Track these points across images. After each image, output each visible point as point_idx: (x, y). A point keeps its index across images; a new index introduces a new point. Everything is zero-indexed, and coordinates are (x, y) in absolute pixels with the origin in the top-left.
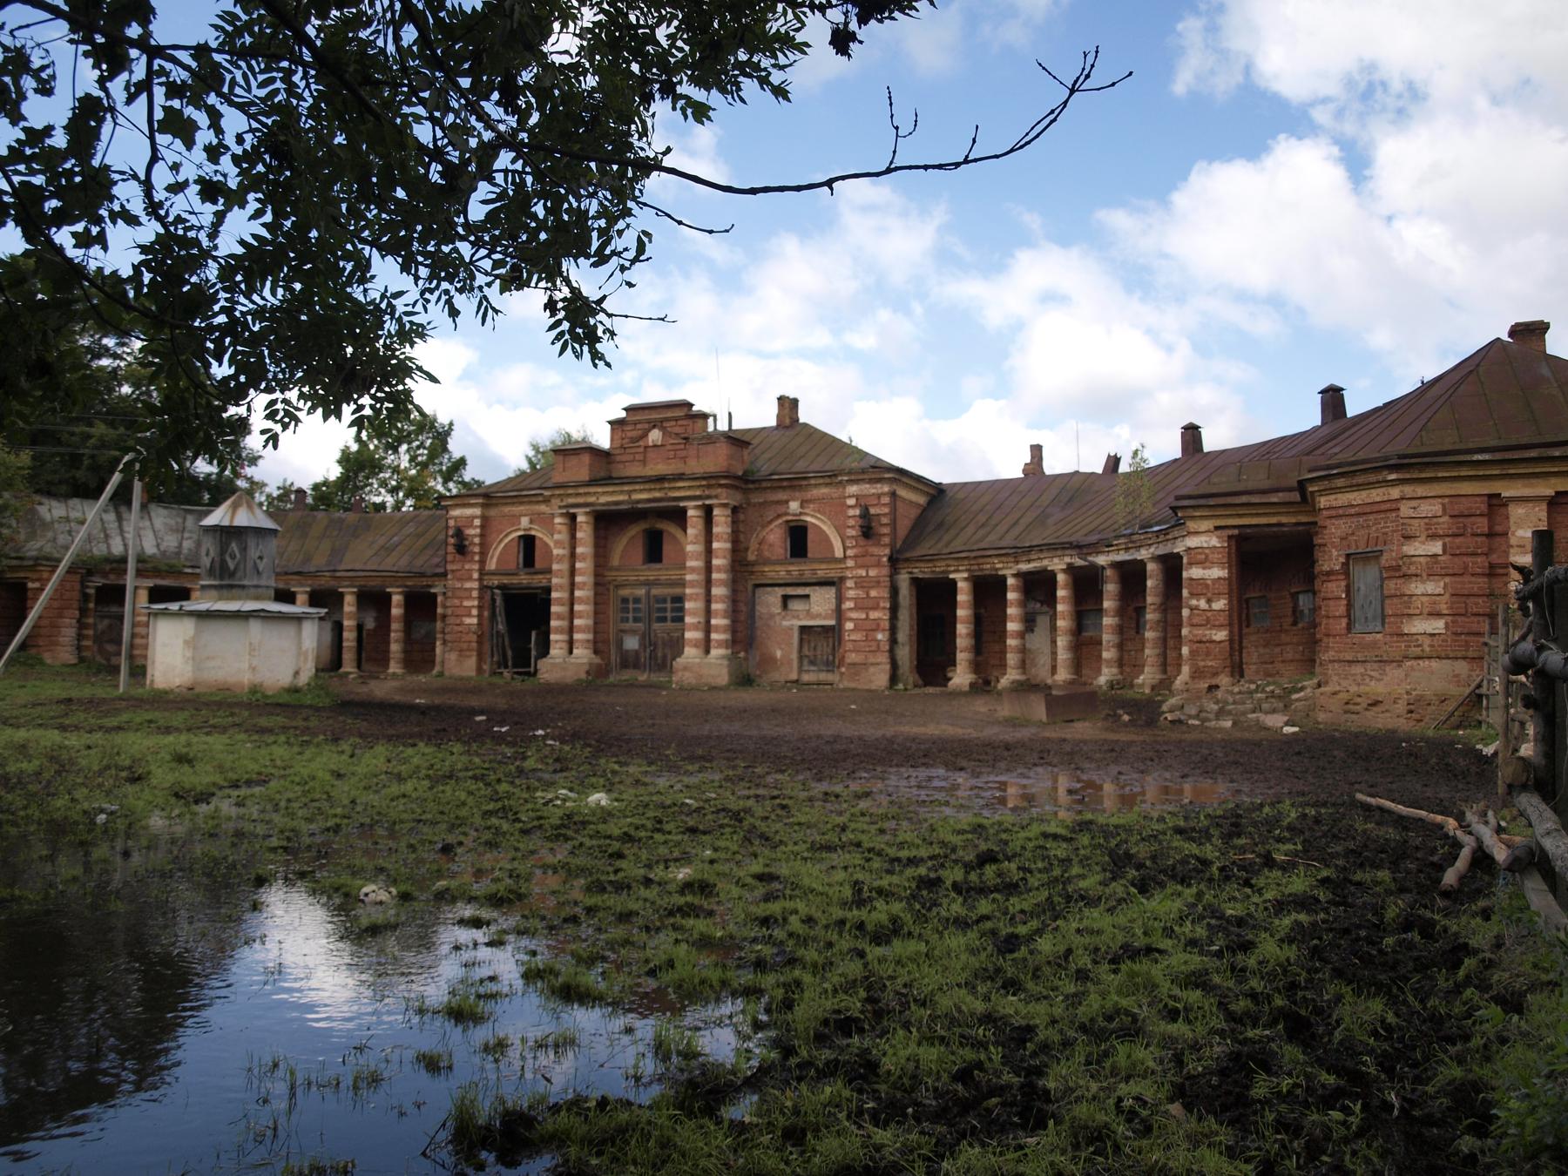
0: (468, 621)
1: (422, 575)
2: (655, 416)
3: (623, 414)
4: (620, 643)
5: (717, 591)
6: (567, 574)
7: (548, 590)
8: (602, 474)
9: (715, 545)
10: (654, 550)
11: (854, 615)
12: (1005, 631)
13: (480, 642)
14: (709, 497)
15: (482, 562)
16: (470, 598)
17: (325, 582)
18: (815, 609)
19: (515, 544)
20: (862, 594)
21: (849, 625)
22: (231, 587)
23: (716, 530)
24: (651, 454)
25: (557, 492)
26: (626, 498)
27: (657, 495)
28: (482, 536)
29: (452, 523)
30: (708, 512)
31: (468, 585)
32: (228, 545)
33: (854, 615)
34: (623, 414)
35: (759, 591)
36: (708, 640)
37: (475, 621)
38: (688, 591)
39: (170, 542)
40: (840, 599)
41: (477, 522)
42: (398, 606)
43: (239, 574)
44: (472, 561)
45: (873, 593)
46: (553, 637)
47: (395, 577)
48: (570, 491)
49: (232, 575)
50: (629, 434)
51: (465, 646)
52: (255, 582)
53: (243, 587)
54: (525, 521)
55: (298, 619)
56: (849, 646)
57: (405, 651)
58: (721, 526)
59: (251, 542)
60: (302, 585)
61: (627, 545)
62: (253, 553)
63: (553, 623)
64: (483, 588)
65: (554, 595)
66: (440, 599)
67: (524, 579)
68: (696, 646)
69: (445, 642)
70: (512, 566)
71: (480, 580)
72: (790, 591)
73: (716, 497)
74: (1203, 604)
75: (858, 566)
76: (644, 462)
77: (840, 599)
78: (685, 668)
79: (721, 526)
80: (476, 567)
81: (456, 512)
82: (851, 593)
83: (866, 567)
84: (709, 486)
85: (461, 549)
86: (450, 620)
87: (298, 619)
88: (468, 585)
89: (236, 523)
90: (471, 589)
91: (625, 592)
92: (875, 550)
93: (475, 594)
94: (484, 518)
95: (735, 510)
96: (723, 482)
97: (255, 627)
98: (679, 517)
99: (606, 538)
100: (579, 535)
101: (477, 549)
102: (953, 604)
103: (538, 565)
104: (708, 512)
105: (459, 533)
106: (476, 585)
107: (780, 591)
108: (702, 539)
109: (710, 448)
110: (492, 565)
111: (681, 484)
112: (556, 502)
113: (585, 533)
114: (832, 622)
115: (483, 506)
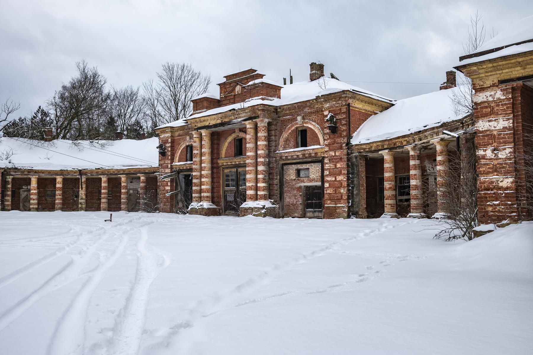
3: (225, 80)
4: (225, 197)
5: (261, 168)
6: (199, 163)
9: (259, 143)
11: (329, 179)
12: (409, 187)
18: (312, 176)
20: (332, 166)
21: (327, 185)
23: (259, 134)
28: (172, 147)
33: (329, 179)
34: (225, 80)
35: (285, 167)
36: (257, 194)
38: (247, 169)
40: (323, 170)
41: (170, 140)
45: (338, 165)
46: (194, 195)
56: (326, 197)
58: (262, 134)
72: (299, 167)
74: (489, 153)
75: (330, 150)
77: (323, 170)
82: (327, 166)
83: (334, 150)
92: (339, 140)
100: (203, 143)
102: (382, 170)
107: (295, 167)
108: (253, 141)
113: (206, 142)
114: (319, 184)
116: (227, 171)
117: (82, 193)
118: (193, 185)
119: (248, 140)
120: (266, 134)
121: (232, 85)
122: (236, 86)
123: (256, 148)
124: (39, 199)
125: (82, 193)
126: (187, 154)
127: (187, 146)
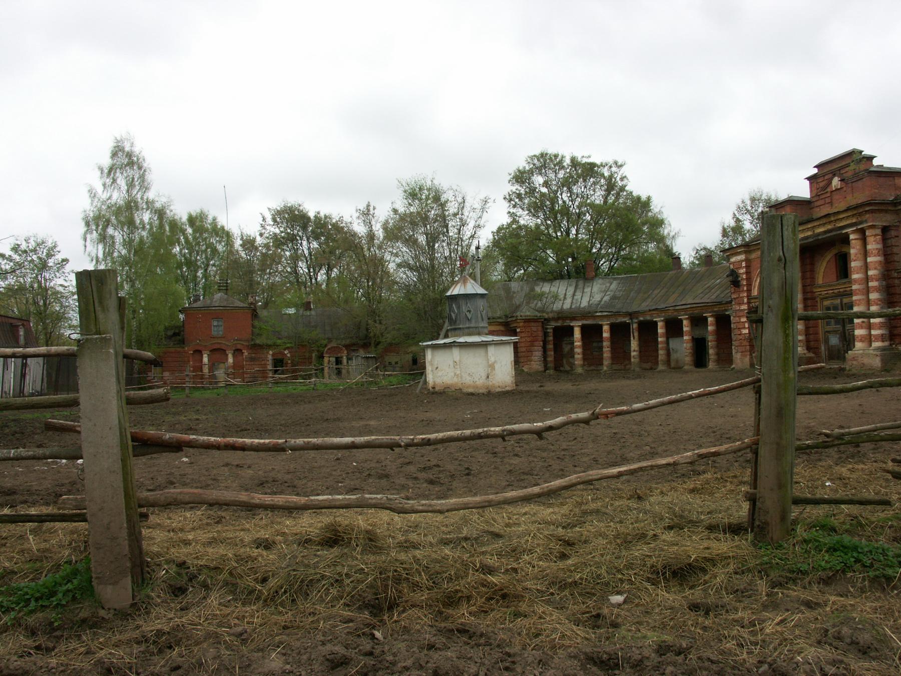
1: (720, 303)
2: (835, 166)
3: (816, 171)
4: (827, 341)
5: (874, 296)
8: (805, 218)
9: (869, 260)
10: (843, 271)
14: (861, 223)
15: (749, 291)
17: (671, 314)
22: (455, 329)
23: (869, 247)
24: (836, 197)
26: (809, 233)
27: (829, 227)
28: (747, 273)
30: (862, 232)
34: (816, 171)
36: (870, 335)
37: (746, 331)
38: (854, 298)
39: (597, 298)
41: (744, 264)
42: (711, 325)
43: (473, 321)
44: (743, 291)
47: (707, 306)
50: (822, 185)
53: (460, 329)
55: (484, 345)
57: (717, 354)
59: (462, 302)
60: (659, 317)
61: (824, 269)
62: (464, 308)
68: (861, 341)
71: (749, 303)
73: (866, 221)
76: (831, 203)
78: (854, 359)
79: (873, 245)
80: (745, 295)
81: (733, 260)
84: (860, 214)
85: (736, 283)
87: (484, 345)
91: (827, 303)
95: (885, 230)
96: (867, 209)
97: (456, 352)
98: (846, 240)
99: (812, 264)
104: (862, 232)
106: (745, 307)
108: (861, 256)
109: (860, 183)
111: (841, 216)
115: (745, 252)
116: (827, 303)
117: (634, 344)
119: (852, 257)
120: (880, 246)
121: (826, 177)
122: (832, 179)
123: (866, 267)
124: (584, 354)
125: (634, 344)
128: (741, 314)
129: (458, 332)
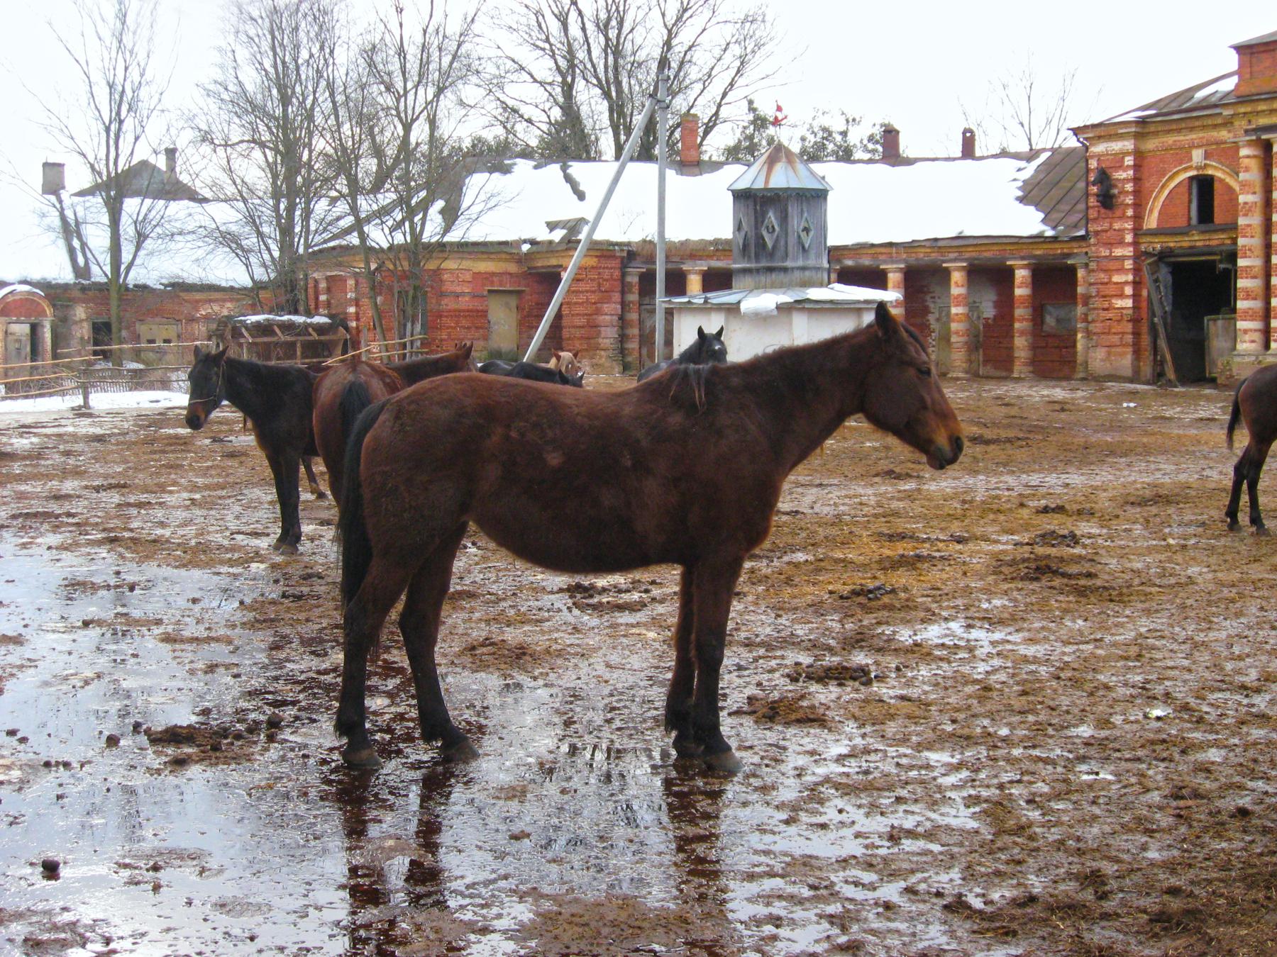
0: (1119, 303)
7: (1232, 256)
13: (1136, 334)
15: (1138, 218)
16: (1121, 270)
19: (1184, 189)
22: (770, 270)
25: (1242, 110)
28: (1137, 180)
29: (1093, 164)
31: (1118, 252)
32: (764, 214)
37: (1129, 303)
41: (1129, 161)
43: (779, 253)
44: (1123, 217)
48: (1262, 107)
49: (771, 255)
51: (1115, 339)
52: (800, 263)
53: (785, 270)
54: (1197, 156)
57: (1034, 347)
62: (796, 223)
63: (1241, 305)
64: (1138, 257)
65: (1241, 262)
66: (1081, 273)
67: (1197, 239)
69: (1089, 334)
70: (1182, 222)
71: (1135, 244)
85: (1107, 201)
86: (1097, 303)
88: (1118, 252)
89: (772, 185)
90: (1123, 258)
93: (1128, 264)
94: (1139, 155)
101: (1129, 200)
103: (1219, 217)
105: (1104, 177)
106: (1129, 251)
110: (1151, 222)
112: (1241, 124)
118: (1240, 295)
126: (1190, 201)
127: (1191, 178)
128: (1116, 265)
129: (781, 277)
